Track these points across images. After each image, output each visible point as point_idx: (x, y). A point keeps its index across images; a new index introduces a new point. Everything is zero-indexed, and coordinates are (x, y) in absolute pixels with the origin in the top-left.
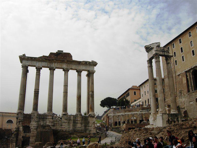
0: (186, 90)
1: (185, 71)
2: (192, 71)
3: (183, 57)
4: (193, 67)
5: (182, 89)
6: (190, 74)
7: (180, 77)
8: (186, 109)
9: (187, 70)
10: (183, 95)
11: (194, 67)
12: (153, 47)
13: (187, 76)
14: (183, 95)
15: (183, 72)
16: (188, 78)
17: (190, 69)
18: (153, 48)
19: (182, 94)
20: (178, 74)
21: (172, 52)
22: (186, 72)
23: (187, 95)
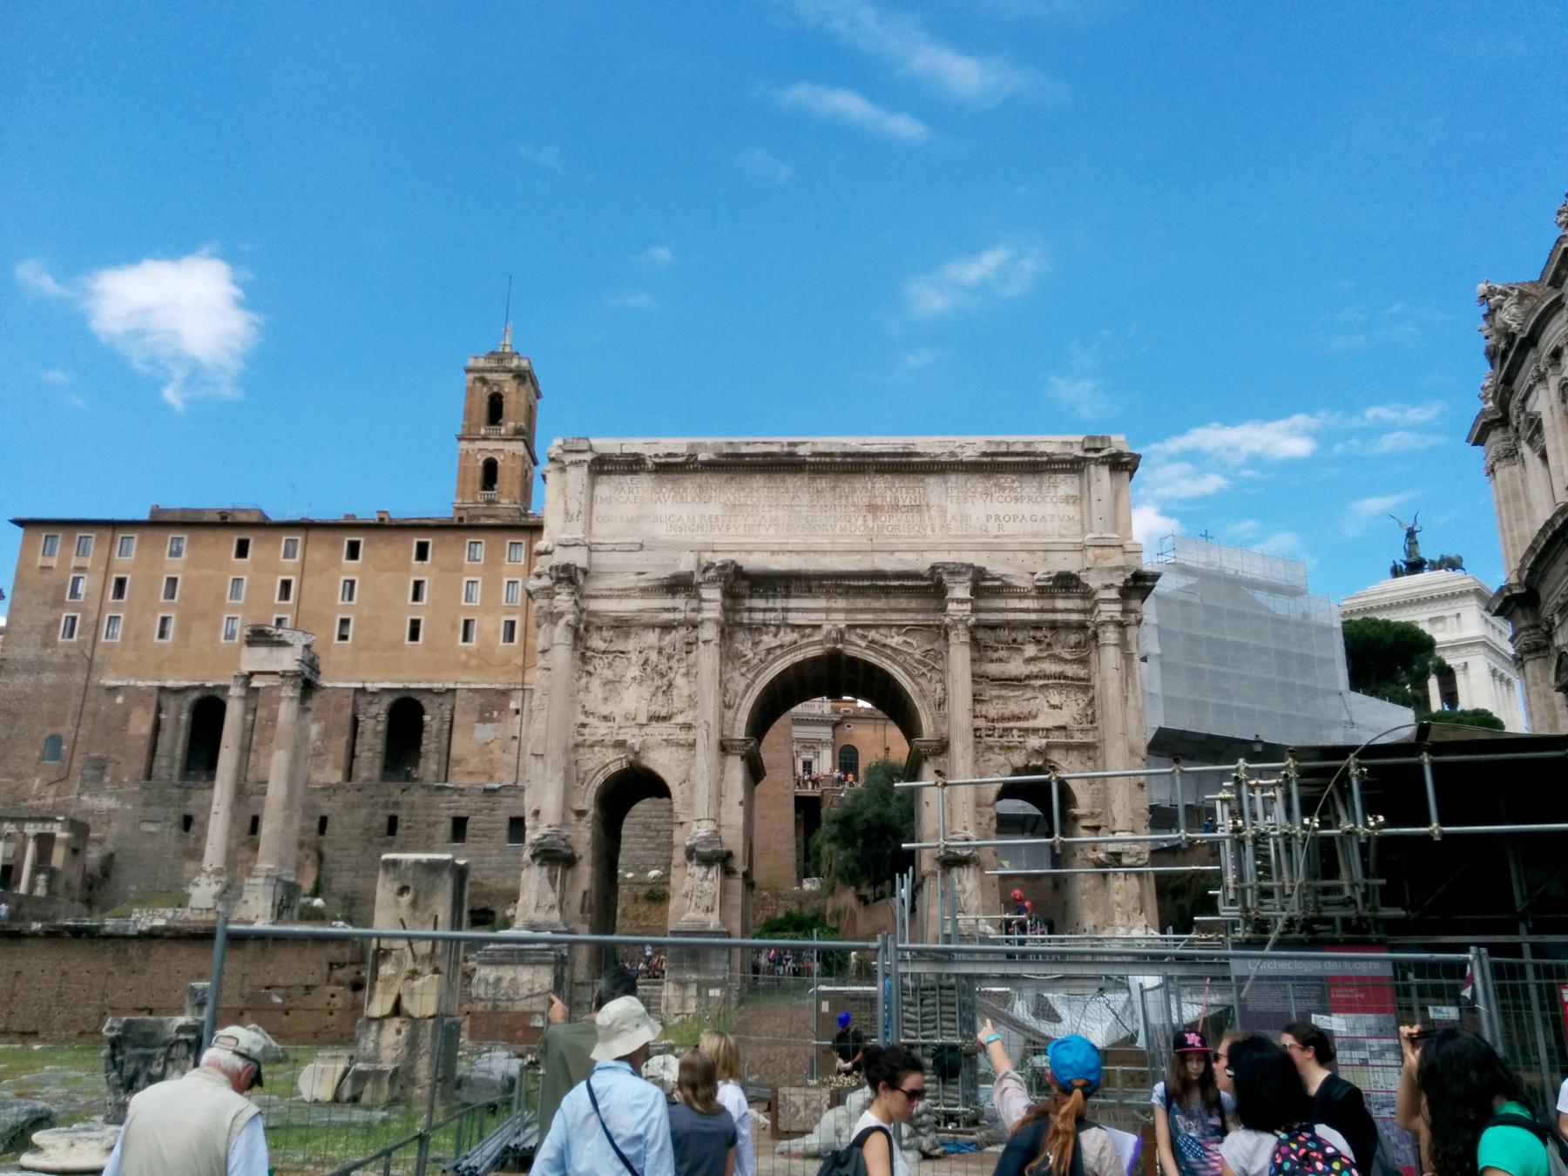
0: (140, 765)
1: (157, 684)
2: (196, 695)
3: (164, 620)
4: (209, 684)
5: (113, 756)
6: (180, 707)
7: (120, 700)
8: (110, 847)
9: (170, 683)
10: (112, 783)
11: (215, 688)
12: (290, 641)
13: (159, 709)
14: (112, 783)
15: (140, 684)
16: (163, 716)
17: (188, 688)
18: (283, 644)
19: (107, 779)
20: (110, 682)
21: (102, 568)
22: (162, 689)
23: (137, 788)
